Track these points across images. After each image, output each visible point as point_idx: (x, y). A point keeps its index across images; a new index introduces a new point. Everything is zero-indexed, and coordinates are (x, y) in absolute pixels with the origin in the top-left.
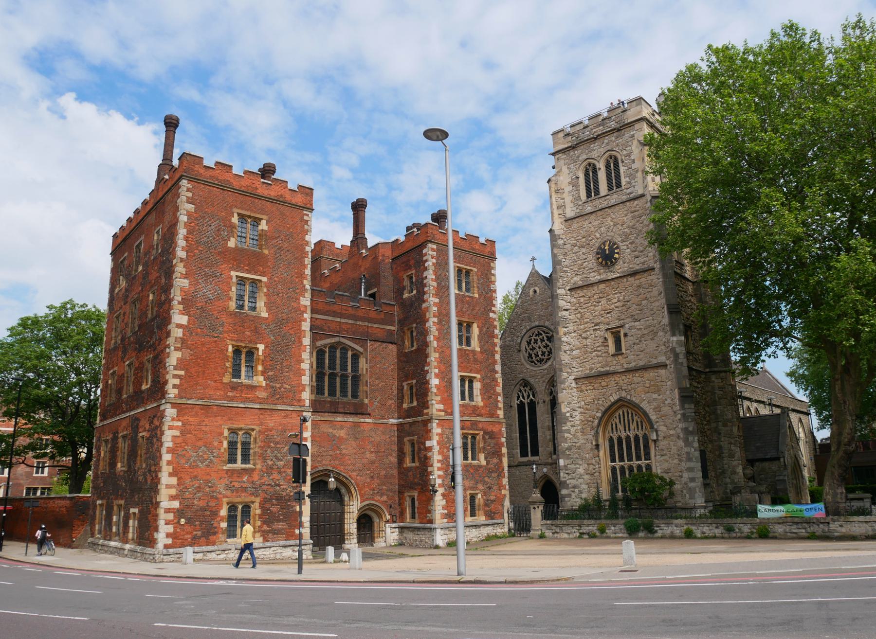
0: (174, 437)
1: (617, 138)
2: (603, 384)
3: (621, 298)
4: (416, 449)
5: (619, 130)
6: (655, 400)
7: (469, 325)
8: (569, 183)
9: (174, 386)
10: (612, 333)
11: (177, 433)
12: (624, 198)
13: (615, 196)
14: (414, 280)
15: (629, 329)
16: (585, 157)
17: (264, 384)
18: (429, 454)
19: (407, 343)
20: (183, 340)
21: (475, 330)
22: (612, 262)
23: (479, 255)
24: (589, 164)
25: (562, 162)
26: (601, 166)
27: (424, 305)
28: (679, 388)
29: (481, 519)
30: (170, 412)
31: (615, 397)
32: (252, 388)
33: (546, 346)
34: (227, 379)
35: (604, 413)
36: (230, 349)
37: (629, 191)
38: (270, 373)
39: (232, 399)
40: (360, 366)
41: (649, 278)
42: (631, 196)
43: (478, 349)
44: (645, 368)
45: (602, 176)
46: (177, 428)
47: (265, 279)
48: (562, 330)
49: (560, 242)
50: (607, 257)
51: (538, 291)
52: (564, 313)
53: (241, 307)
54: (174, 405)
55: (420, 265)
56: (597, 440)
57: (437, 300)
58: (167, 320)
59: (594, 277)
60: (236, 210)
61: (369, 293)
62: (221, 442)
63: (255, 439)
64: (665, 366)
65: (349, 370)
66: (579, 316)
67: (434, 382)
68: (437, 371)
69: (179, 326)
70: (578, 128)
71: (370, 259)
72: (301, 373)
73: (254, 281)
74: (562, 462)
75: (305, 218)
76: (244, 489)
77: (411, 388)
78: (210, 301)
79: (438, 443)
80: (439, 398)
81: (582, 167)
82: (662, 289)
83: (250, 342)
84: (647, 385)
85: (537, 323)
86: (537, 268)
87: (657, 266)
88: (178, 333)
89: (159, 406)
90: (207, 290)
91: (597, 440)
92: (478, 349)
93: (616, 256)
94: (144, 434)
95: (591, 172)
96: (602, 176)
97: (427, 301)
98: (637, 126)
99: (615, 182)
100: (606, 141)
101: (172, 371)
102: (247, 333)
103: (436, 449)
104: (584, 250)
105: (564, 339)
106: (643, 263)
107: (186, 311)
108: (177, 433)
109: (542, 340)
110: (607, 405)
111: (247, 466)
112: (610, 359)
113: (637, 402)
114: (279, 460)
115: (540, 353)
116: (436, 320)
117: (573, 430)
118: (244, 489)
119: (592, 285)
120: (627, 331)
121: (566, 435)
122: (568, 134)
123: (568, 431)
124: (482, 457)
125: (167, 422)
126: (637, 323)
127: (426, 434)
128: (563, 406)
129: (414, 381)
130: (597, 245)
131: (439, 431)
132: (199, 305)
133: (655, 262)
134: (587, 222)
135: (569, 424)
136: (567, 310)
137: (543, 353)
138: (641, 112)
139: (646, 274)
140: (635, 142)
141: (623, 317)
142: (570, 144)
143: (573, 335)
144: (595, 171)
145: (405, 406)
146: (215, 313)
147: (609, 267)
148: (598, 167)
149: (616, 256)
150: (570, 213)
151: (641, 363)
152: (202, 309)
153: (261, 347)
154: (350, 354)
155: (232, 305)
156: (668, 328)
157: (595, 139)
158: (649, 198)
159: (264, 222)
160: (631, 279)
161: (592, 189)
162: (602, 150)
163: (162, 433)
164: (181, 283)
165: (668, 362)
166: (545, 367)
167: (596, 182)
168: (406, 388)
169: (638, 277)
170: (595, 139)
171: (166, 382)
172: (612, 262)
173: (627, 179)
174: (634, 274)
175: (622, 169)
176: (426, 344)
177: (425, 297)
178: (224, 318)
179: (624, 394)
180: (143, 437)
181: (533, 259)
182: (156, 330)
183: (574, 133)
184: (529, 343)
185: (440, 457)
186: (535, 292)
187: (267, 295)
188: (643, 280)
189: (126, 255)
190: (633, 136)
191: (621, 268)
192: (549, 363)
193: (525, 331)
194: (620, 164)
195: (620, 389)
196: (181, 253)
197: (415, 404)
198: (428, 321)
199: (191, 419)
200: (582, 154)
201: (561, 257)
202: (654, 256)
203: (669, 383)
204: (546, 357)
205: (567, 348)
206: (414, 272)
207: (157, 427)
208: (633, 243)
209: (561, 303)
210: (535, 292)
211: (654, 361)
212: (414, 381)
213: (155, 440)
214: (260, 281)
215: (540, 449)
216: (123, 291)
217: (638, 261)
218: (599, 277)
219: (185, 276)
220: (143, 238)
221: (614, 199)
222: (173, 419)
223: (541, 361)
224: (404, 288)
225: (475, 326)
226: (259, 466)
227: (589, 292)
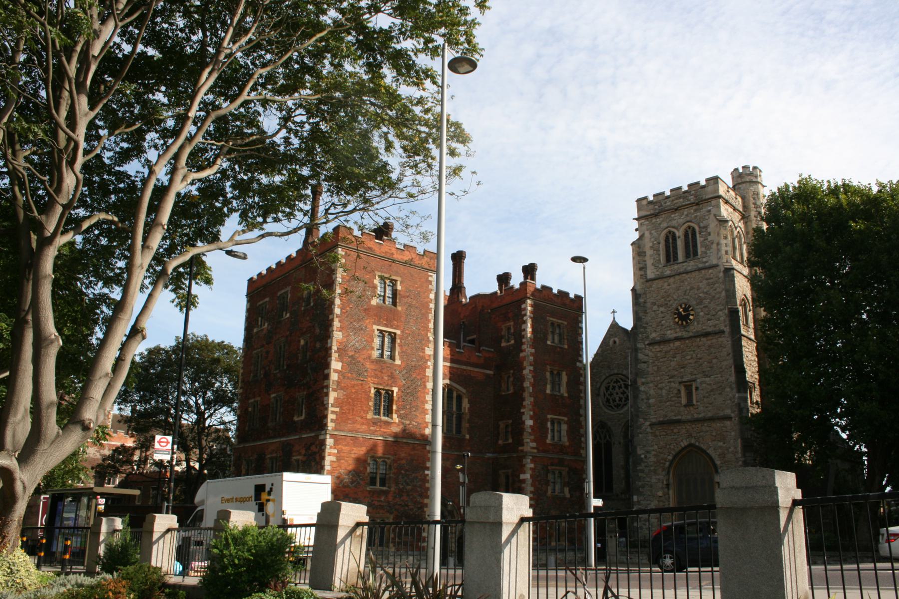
0: (332, 462)
1: (696, 210)
2: (675, 431)
3: (694, 355)
4: (511, 480)
5: (697, 204)
6: (720, 447)
7: (559, 374)
8: (651, 247)
9: (332, 420)
10: (685, 386)
11: (334, 459)
12: (701, 266)
13: (692, 263)
14: (512, 331)
15: (701, 383)
16: (665, 225)
17: (397, 421)
18: (523, 485)
19: (504, 386)
20: (338, 383)
21: (565, 378)
22: (687, 322)
23: (567, 310)
24: (670, 232)
25: (645, 228)
26: (680, 233)
27: (522, 355)
28: (742, 439)
29: (565, 543)
30: (329, 441)
31: (684, 443)
32: (388, 424)
33: (623, 393)
34: (370, 415)
35: (675, 457)
36: (373, 391)
37: (704, 260)
38: (402, 412)
39: (373, 433)
40: (463, 405)
41: (720, 339)
42: (707, 264)
43: (566, 395)
44: (712, 419)
45: (680, 244)
46: (334, 454)
47: (398, 332)
48: (640, 381)
49: (642, 300)
50: (683, 318)
51: (618, 342)
52: (643, 366)
53: (382, 355)
54: (332, 436)
55: (519, 319)
56: (668, 480)
57: (533, 351)
58: (328, 365)
59: (670, 334)
60: (378, 273)
61: (468, 338)
62: (366, 468)
63: (390, 466)
64: (729, 418)
65: (454, 409)
66: (655, 368)
67: (529, 423)
68: (532, 413)
69: (336, 371)
70: (660, 197)
71: (470, 308)
72: (425, 412)
73: (390, 333)
74: (635, 498)
75: (430, 279)
76: (382, 507)
77: (507, 426)
78: (357, 351)
79: (531, 476)
80: (532, 437)
82: (730, 351)
83: (387, 385)
84: (714, 434)
85: (616, 371)
86: (617, 320)
87: (727, 330)
88: (334, 377)
89: (317, 436)
90: (355, 341)
91: (668, 480)
92: (566, 395)
93: (691, 317)
94: (299, 457)
95: (670, 239)
96: (680, 244)
97: (525, 351)
98: (714, 202)
99: (691, 251)
100: (685, 213)
101: (331, 409)
102: (386, 378)
103: (529, 482)
104: (662, 309)
105: (642, 388)
106: (715, 326)
107: (341, 359)
108: (334, 459)
109: (620, 387)
110: (677, 450)
111: (384, 488)
112: (682, 409)
113: (704, 448)
114: (408, 484)
115: (617, 399)
116: (532, 368)
117: (646, 470)
118: (382, 507)
119: (669, 341)
121: (640, 474)
122: (651, 202)
123: (642, 471)
124: (566, 490)
125: (328, 450)
126: (707, 379)
127: (521, 469)
128: (638, 449)
129: (510, 421)
130: (674, 306)
131: (532, 466)
132: (350, 353)
133: (726, 326)
134: (666, 284)
135: (643, 465)
136: (645, 362)
137: (620, 399)
138: (717, 190)
139: (717, 336)
140: (712, 216)
141: (695, 372)
142: (652, 212)
143: (651, 385)
144: (674, 238)
145: (500, 442)
146: (361, 360)
147: (685, 327)
149: (691, 317)
150: (650, 274)
151: (710, 414)
152: (352, 357)
153: (395, 390)
154: (455, 394)
155: (376, 354)
156: (734, 386)
157: (676, 210)
158: (722, 269)
159: (399, 283)
160: (704, 339)
161: (671, 256)
162: (681, 221)
163: (323, 458)
164: (337, 335)
165: (733, 415)
166: (622, 412)
168: (502, 425)
169: (710, 338)
170: (676, 210)
171: (326, 417)
172: (687, 322)
173: (703, 249)
174: (706, 334)
176: (523, 389)
177: (524, 347)
178: (369, 365)
179: (693, 441)
180: (297, 461)
181: (614, 312)
182: (309, 371)
184: (607, 389)
185: (532, 489)
186: (615, 342)
187: (400, 346)
188: (714, 341)
189: (267, 299)
190: (709, 211)
191: (695, 328)
192: (626, 408)
193: (604, 377)
194: (698, 235)
195: (690, 436)
196: (337, 311)
197: (510, 441)
198: (525, 368)
199: (344, 448)
200: (663, 222)
201: (641, 314)
202: (725, 321)
203: (733, 433)
204: (623, 403)
205: (644, 397)
206: (512, 323)
207: (315, 453)
209: (641, 356)
210: (615, 342)
211: (721, 414)
212: (510, 421)
213: (313, 464)
214: (395, 334)
215: (614, 486)
216: (265, 332)
217: (710, 323)
218: (675, 335)
219: (341, 329)
220: (289, 288)
221: (691, 265)
222: (331, 447)
223: (617, 406)
224: (502, 337)
225: (564, 374)
226: (393, 489)
227: (665, 348)
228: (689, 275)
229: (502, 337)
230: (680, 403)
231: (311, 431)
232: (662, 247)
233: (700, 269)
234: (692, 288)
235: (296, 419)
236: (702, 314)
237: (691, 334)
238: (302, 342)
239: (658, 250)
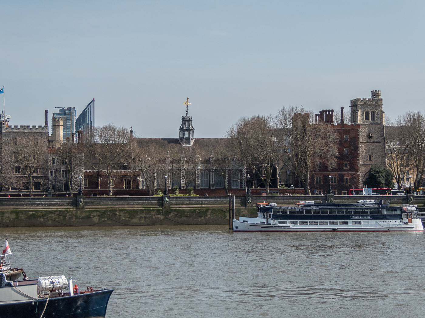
12: (375, 123)
37: (376, 121)
120: (373, 155)
161: (367, 118)
174: (376, 142)
190: (379, 108)
208: (376, 135)
217: (377, 139)
228: (372, 125)
230: (368, 160)
231: (352, 172)
233: (375, 124)
234: (373, 129)
235: (344, 168)
236: (375, 136)
237: (372, 142)
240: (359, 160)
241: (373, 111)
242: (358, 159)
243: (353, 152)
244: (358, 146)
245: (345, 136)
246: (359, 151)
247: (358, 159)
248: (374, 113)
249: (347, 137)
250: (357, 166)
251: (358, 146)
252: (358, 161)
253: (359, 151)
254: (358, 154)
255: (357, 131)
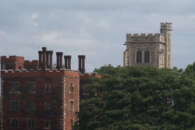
8: (131, 55)
16: (137, 47)
25: (129, 46)
26: (143, 53)
47: (74, 100)
70: (136, 36)
81: (136, 51)
95: (139, 53)
148: (142, 53)
153: (73, 119)
167: (141, 57)
175: (150, 57)
183: (135, 37)
190: (155, 46)
194: (150, 55)
224: (83, 91)
229: (83, 91)
232: (136, 56)
238: (46, 104)
239: (134, 57)
240: (62, 117)
241: (147, 51)
242: (61, 116)
243: (56, 106)
244: (62, 99)
245: (46, 86)
246: (62, 105)
247: (61, 116)
248: (148, 53)
249: (48, 87)
250: (61, 125)
251: (62, 99)
252: (61, 119)
253: (62, 105)
254: (62, 110)
255: (61, 79)
